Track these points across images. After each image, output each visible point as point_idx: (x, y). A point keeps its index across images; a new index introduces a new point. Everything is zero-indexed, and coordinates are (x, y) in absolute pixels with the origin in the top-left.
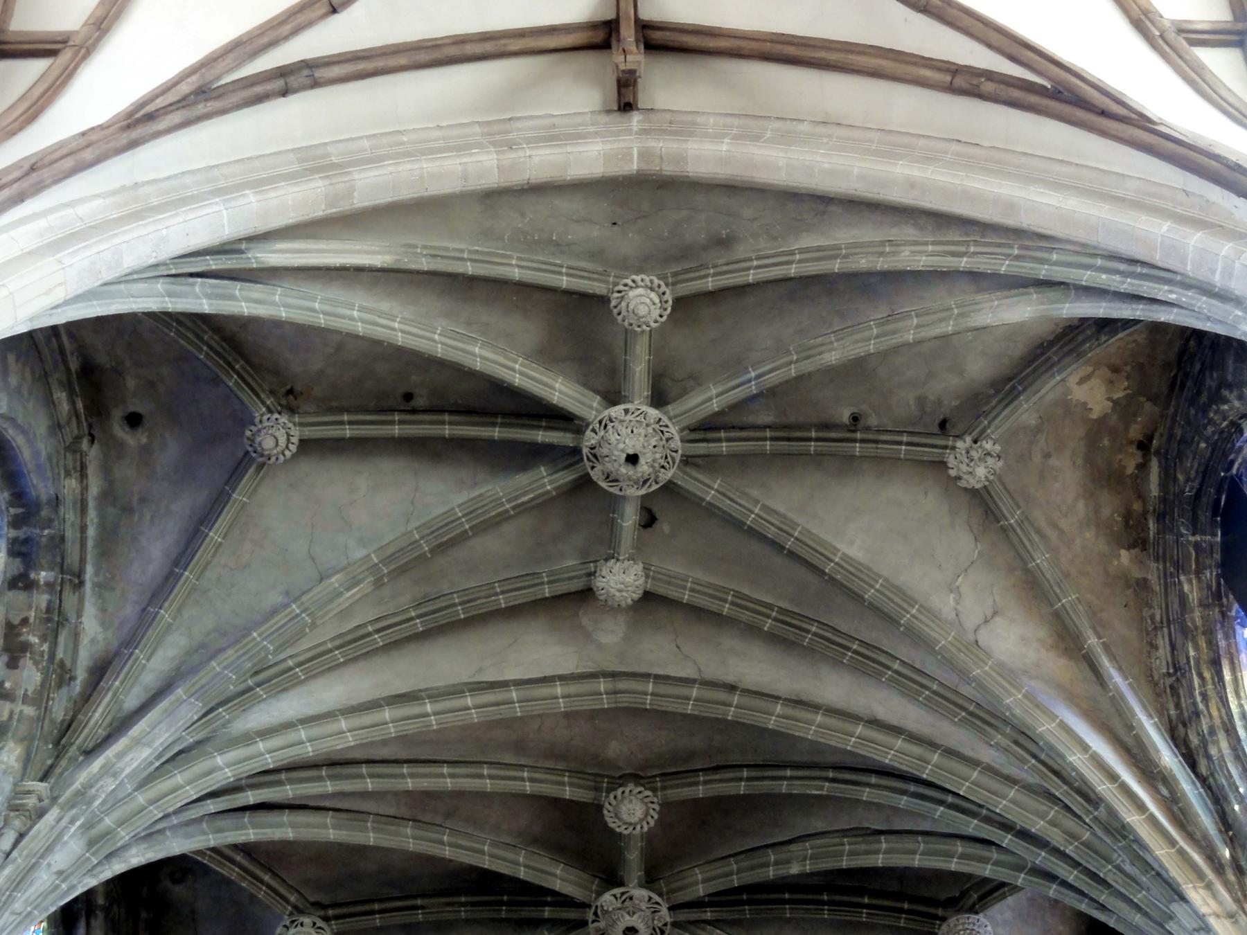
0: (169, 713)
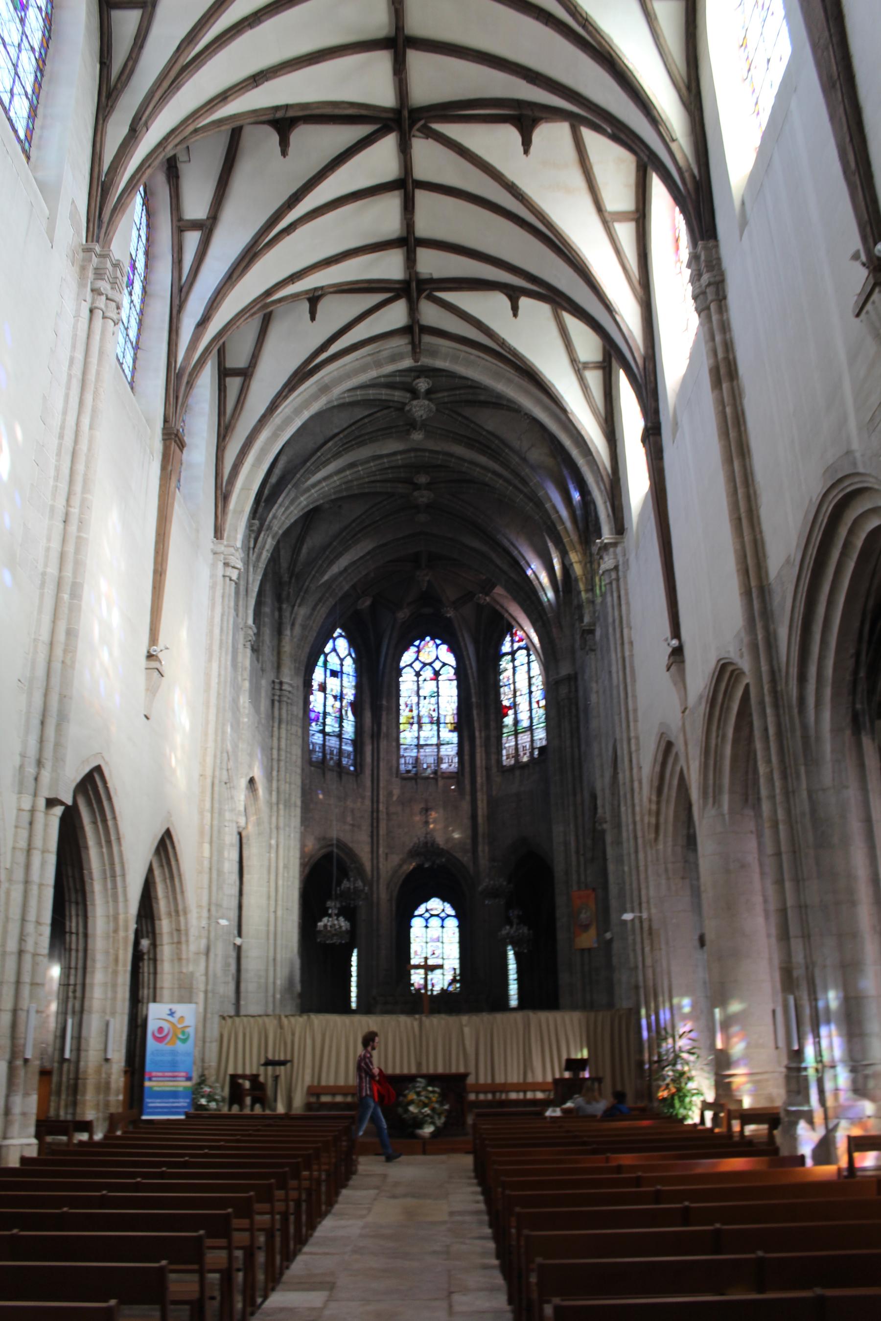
0: (287, 494)
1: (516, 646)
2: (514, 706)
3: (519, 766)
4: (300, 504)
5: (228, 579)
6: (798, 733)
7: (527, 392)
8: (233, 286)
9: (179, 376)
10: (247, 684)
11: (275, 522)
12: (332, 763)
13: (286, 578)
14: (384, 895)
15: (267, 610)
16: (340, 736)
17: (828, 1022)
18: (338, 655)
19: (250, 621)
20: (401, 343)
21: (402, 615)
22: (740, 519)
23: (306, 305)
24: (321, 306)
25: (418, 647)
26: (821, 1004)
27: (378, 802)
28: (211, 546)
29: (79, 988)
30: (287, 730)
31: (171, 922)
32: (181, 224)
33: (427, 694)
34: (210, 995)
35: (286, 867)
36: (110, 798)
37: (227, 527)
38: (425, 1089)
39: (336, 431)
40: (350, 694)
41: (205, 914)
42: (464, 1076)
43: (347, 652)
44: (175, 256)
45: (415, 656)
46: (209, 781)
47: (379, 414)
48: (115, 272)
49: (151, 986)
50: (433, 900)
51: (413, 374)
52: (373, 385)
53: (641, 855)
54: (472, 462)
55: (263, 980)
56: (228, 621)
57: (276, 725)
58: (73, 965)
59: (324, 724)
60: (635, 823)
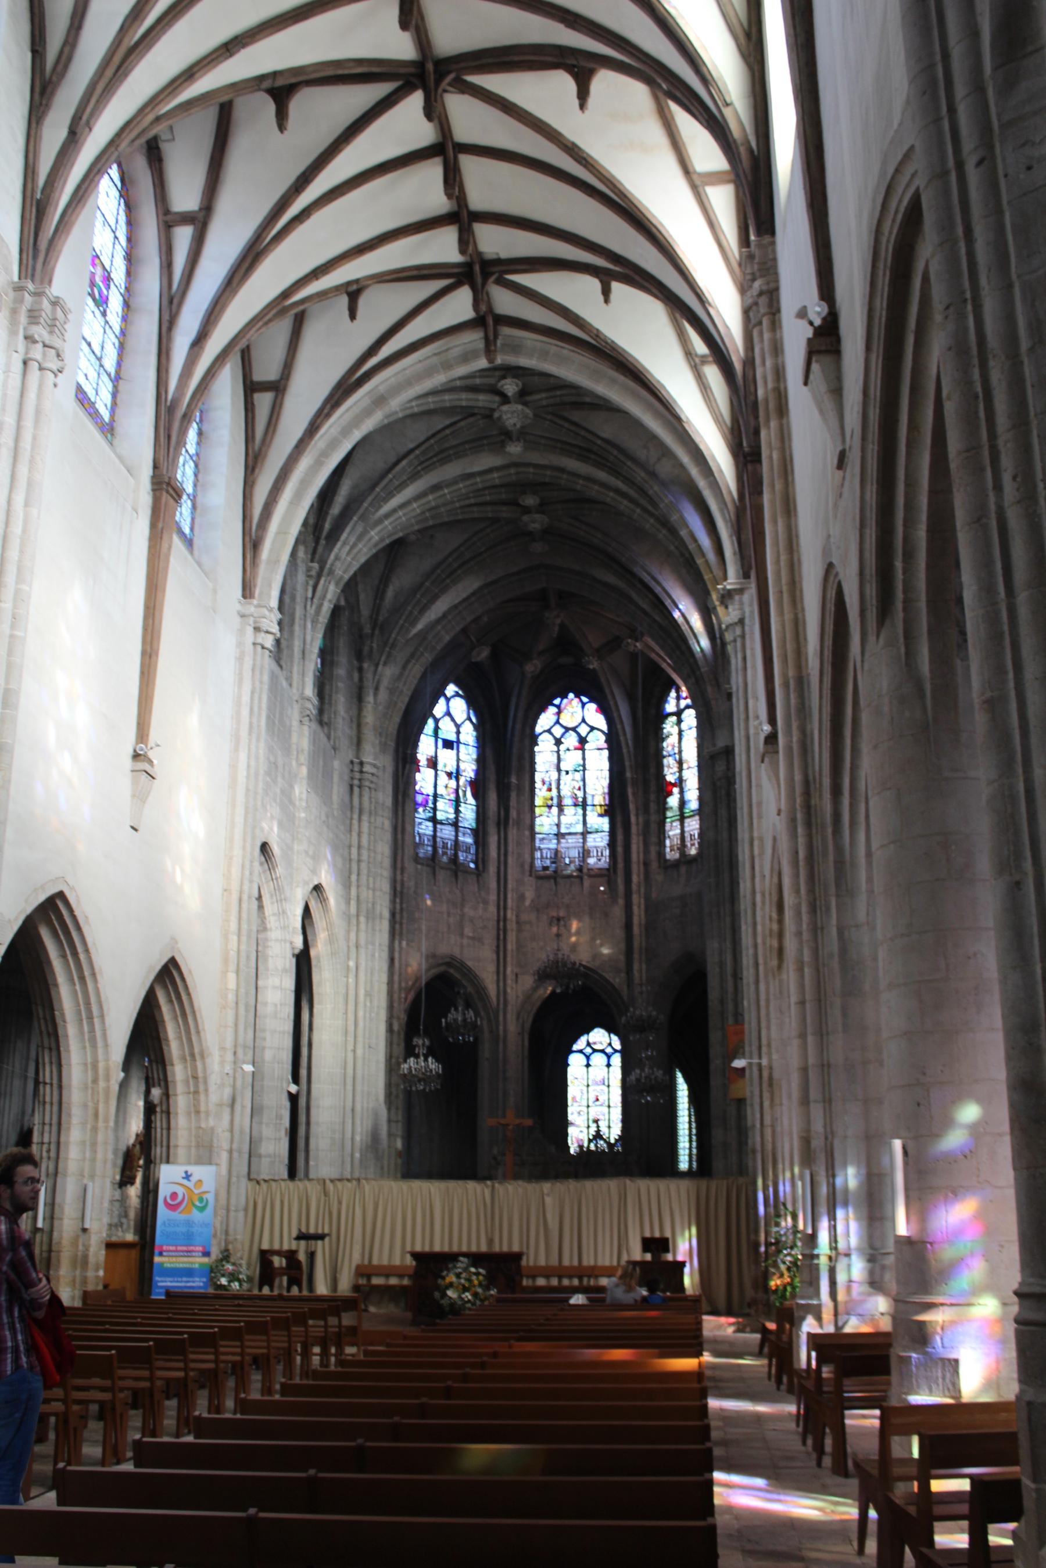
0: (353, 529)
1: (683, 703)
2: (680, 782)
3: (685, 860)
4: (370, 540)
5: (259, 648)
6: (831, 858)
7: (635, 396)
8: (235, 292)
9: (171, 410)
10: (304, 771)
11: (338, 564)
12: (445, 859)
13: (367, 630)
14: (513, 1027)
15: (341, 671)
16: (455, 824)
17: (845, 1204)
18: (453, 720)
19: (310, 691)
20: (474, 338)
21: (532, 667)
22: (781, 592)
23: (344, 300)
24: (362, 302)
25: (558, 707)
26: (839, 1181)
27: (505, 908)
28: (238, 607)
29: (53, 1147)
30: (370, 822)
31: (186, 1068)
32: (169, 218)
33: (570, 768)
34: (235, 1155)
35: (368, 994)
36: (79, 928)
37: (259, 581)
38: (466, 1269)
39: (411, 446)
40: (469, 770)
41: (229, 1057)
42: (517, 1257)
43: (465, 716)
44: (164, 258)
45: (555, 718)
46: (235, 897)
47: (462, 424)
48: (54, 311)
49: (165, 1143)
50: (596, 1030)
51: (497, 373)
52: (448, 389)
53: (762, 987)
54: (588, 479)
55: (337, 1136)
56: (260, 698)
57: (356, 816)
58: (47, 1120)
59: (435, 809)
60: (756, 946)
